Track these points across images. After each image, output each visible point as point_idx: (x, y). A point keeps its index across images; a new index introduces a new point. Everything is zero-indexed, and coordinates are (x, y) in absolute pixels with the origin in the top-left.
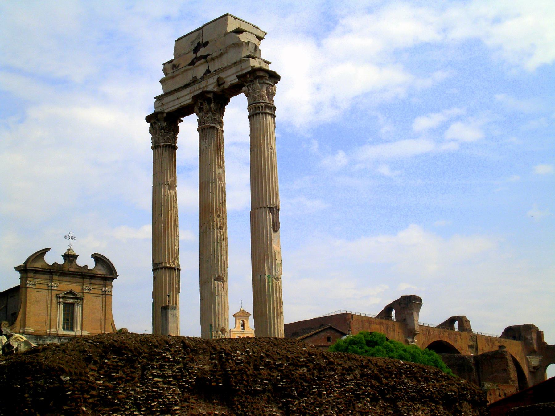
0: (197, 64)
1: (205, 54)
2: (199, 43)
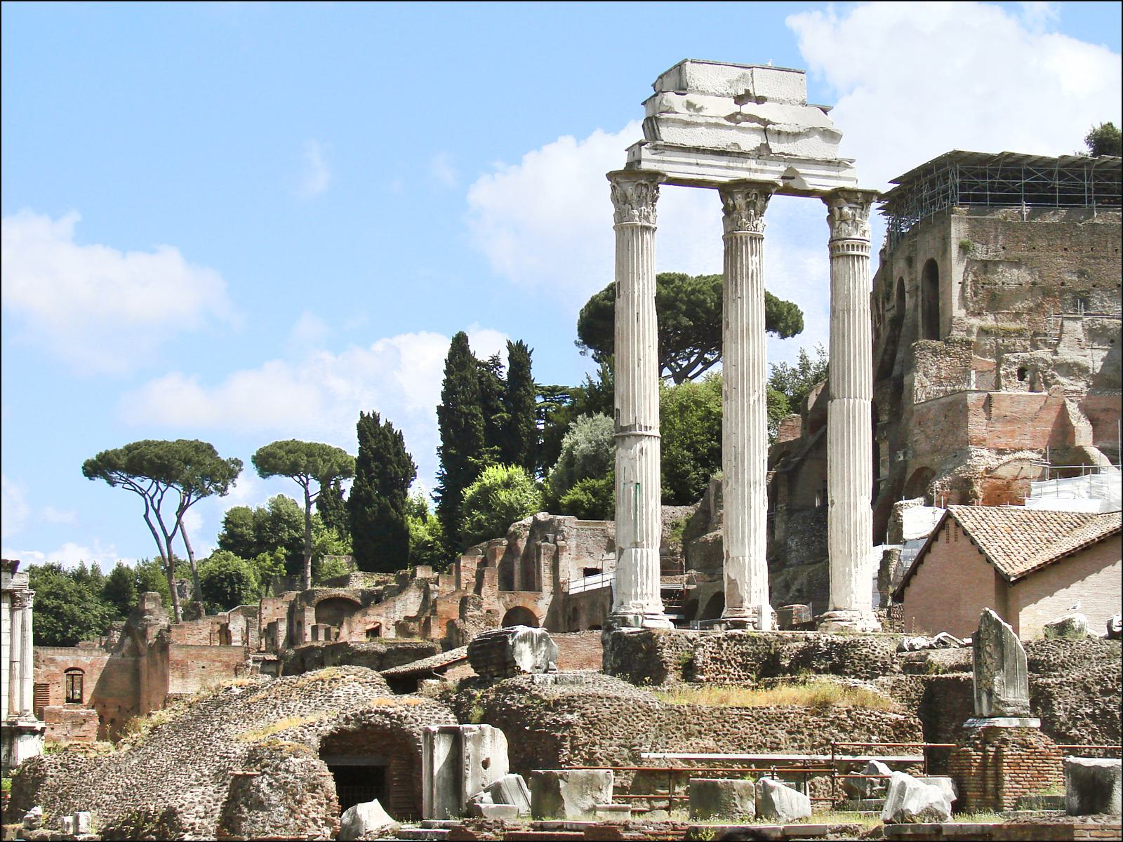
0: (743, 124)
1: (767, 118)
2: (747, 91)
